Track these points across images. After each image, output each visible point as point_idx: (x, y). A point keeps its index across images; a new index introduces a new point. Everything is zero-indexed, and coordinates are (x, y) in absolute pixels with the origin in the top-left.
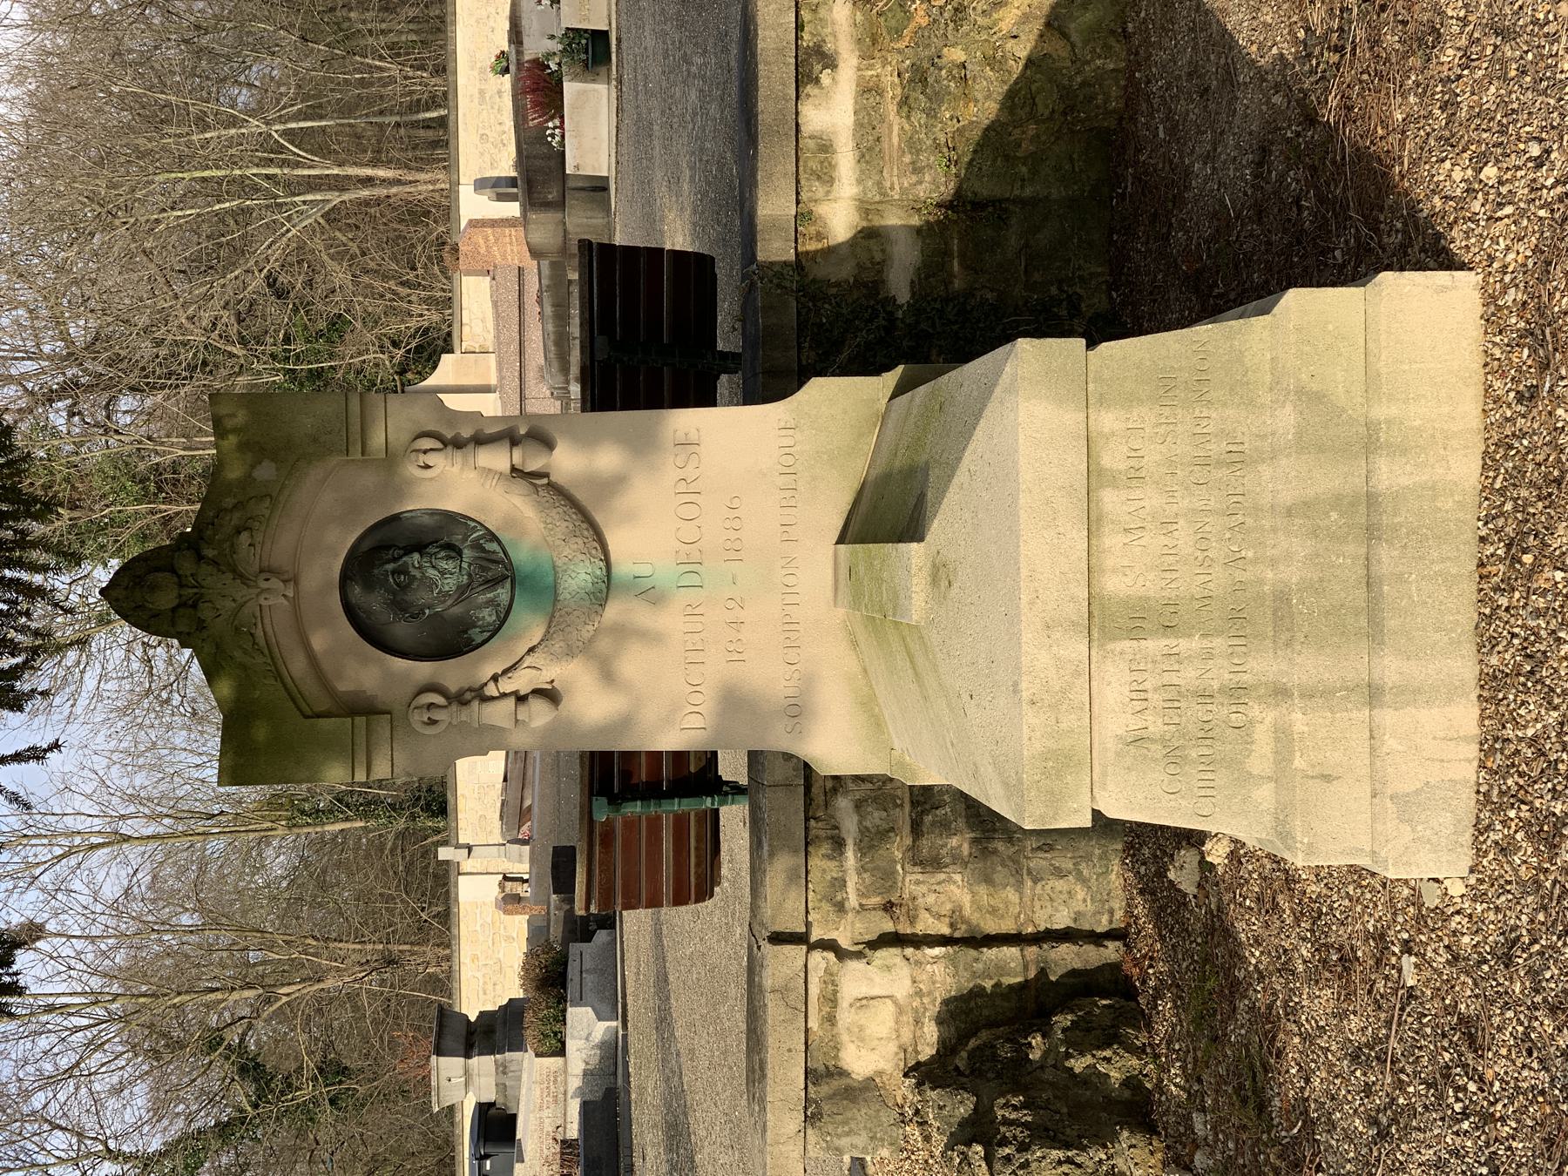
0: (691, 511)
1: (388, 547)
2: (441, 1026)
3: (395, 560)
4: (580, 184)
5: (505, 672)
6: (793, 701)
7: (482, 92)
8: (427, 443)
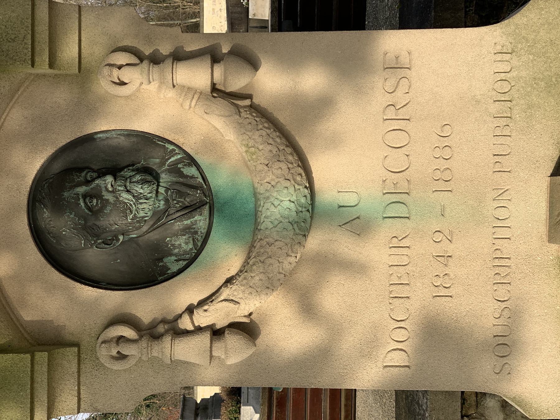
0: (399, 139)
1: (81, 170)
2: (184, 405)
3: (87, 182)
4: (255, 25)
5: (202, 303)
6: (502, 340)
7: (213, 9)
8: (122, 58)
